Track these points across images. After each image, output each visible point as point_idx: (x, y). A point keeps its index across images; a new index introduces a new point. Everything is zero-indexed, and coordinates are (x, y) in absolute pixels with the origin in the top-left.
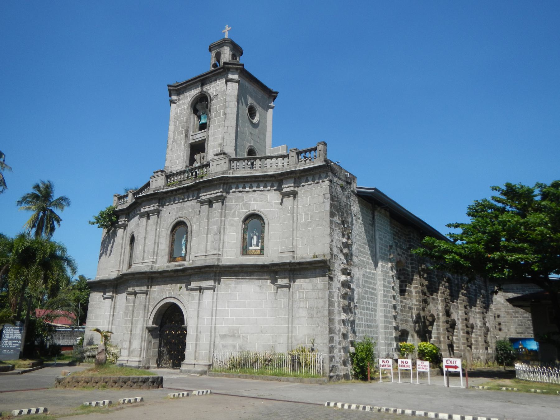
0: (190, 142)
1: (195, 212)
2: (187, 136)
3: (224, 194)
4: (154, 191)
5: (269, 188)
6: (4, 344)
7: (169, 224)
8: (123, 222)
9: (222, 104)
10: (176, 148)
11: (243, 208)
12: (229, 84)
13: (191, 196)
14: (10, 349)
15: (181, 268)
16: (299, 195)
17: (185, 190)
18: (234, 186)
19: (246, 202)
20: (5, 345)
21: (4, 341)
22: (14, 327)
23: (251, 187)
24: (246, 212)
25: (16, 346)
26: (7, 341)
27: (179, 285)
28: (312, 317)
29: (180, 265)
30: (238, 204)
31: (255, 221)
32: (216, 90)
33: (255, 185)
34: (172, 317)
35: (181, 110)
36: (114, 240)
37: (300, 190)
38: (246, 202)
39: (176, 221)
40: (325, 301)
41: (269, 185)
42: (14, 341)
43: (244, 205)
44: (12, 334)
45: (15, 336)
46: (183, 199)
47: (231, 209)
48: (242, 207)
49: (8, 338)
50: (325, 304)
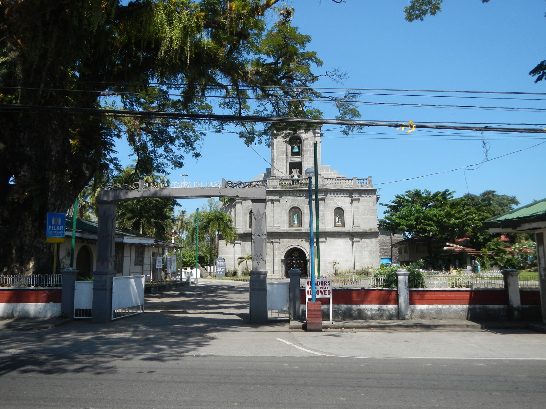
0: (289, 161)
1: (305, 203)
2: (287, 158)
3: (325, 197)
4: (273, 188)
5: (345, 195)
7: (287, 207)
8: (239, 201)
12: (317, 135)
13: (301, 194)
14: (221, 271)
15: (300, 231)
16: (360, 200)
17: (299, 191)
18: (329, 193)
23: (337, 194)
24: (335, 206)
27: (300, 240)
28: (371, 254)
29: (298, 230)
31: (339, 210)
33: (339, 193)
36: (231, 211)
37: (361, 198)
39: (292, 206)
40: (377, 248)
41: (345, 193)
43: (334, 203)
46: (296, 195)
47: (328, 204)
50: (377, 249)
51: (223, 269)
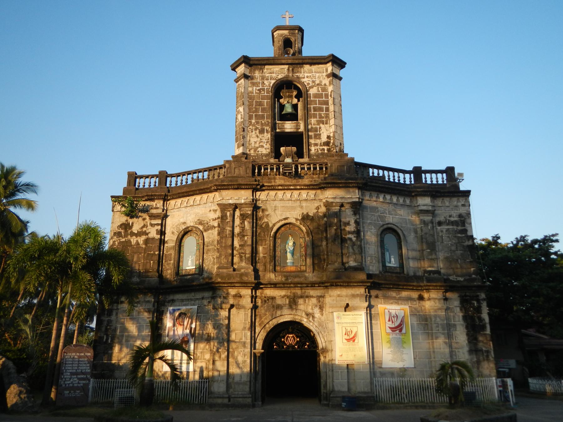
6: (65, 381)
9: (324, 99)
10: (256, 133)
11: (379, 220)
14: (73, 388)
19: (381, 213)
20: (66, 382)
21: (65, 377)
22: (77, 354)
25: (83, 383)
26: (69, 377)
30: (373, 215)
32: (313, 81)
34: (283, 340)
35: (259, 90)
38: (381, 213)
42: (79, 376)
43: (379, 216)
44: (76, 365)
45: (81, 368)
48: (377, 219)
49: (70, 371)
51: (80, 379)
